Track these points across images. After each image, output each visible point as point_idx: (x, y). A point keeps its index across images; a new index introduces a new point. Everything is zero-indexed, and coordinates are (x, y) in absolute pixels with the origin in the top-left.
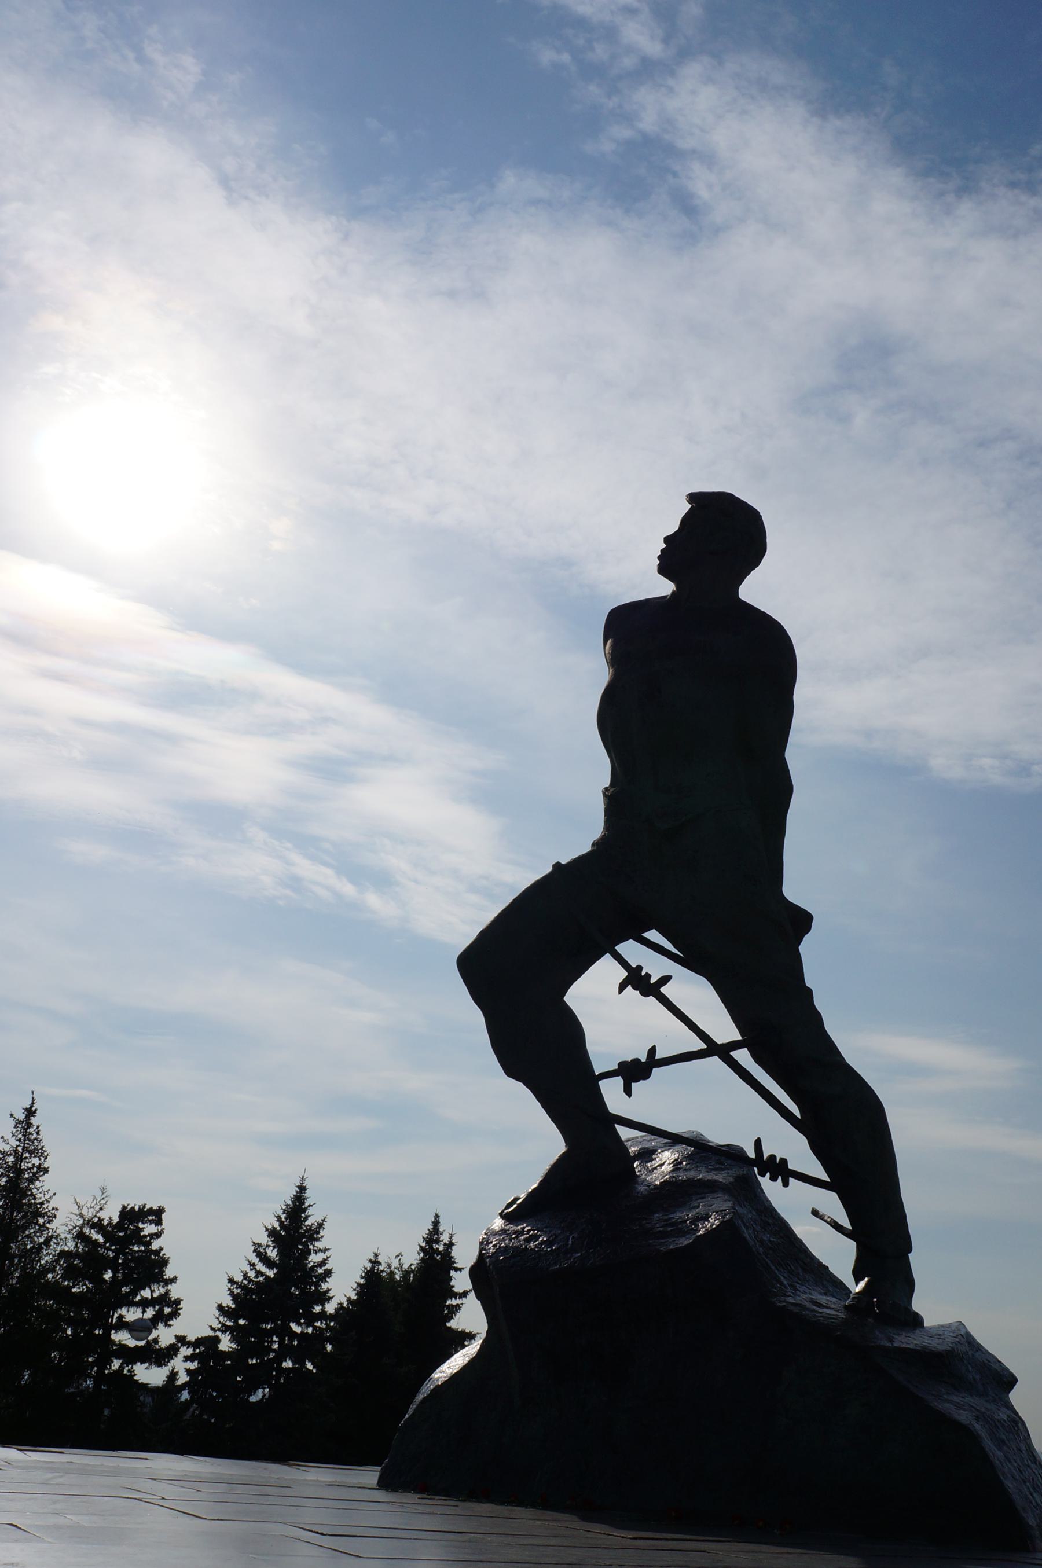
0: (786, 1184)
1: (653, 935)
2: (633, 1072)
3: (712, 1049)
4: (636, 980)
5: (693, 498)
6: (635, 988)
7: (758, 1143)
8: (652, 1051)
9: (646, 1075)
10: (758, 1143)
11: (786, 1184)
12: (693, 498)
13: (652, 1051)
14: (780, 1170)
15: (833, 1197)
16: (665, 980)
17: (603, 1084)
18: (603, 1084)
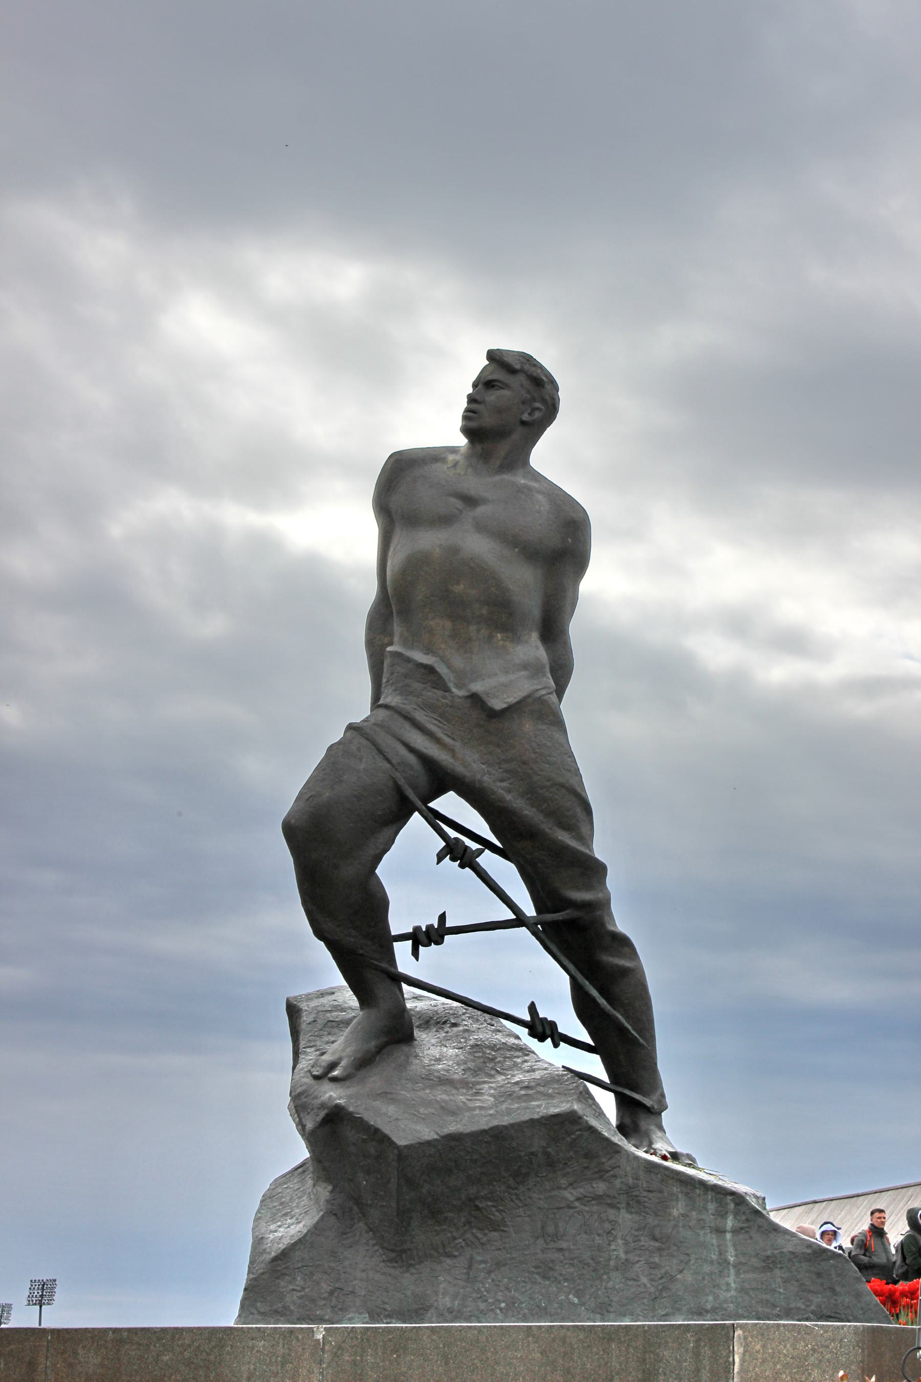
0: (556, 1045)
1: (450, 804)
2: (423, 938)
3: (519, 921)
4: (455, 852)
5: (494, 356)
6: (453, 859)
7: (532, 1008)
8: (442, 918)
9: (439, 942)
10: (532, 1008)
11: (556, 1045)
12: (494, 356)
13: (442, 918)
14: (543, 1029)
15: (596, 1058)
16: (480, 852)
17: (397, 945)
18: (397, 945)
